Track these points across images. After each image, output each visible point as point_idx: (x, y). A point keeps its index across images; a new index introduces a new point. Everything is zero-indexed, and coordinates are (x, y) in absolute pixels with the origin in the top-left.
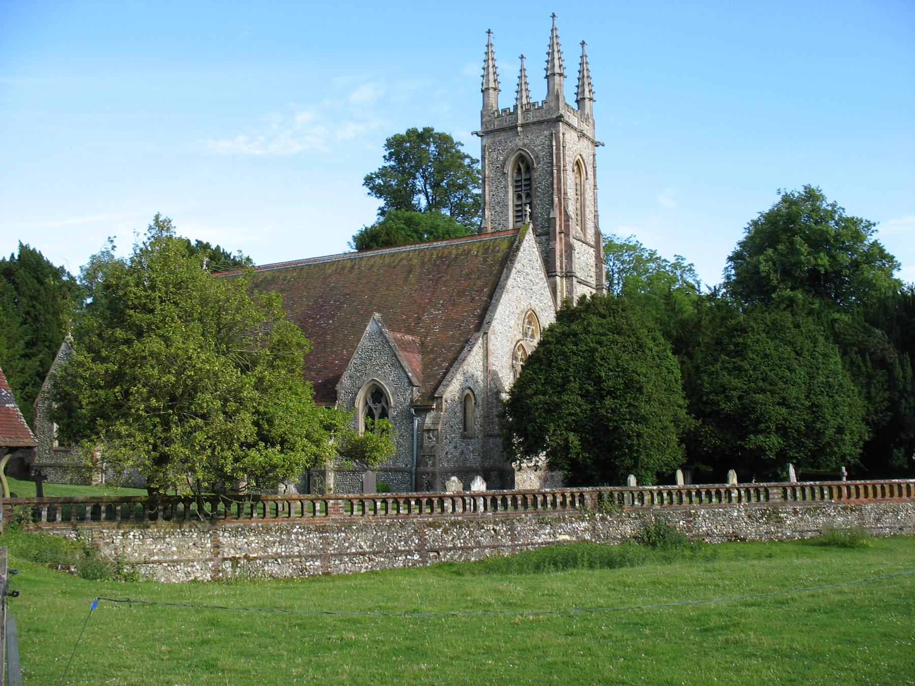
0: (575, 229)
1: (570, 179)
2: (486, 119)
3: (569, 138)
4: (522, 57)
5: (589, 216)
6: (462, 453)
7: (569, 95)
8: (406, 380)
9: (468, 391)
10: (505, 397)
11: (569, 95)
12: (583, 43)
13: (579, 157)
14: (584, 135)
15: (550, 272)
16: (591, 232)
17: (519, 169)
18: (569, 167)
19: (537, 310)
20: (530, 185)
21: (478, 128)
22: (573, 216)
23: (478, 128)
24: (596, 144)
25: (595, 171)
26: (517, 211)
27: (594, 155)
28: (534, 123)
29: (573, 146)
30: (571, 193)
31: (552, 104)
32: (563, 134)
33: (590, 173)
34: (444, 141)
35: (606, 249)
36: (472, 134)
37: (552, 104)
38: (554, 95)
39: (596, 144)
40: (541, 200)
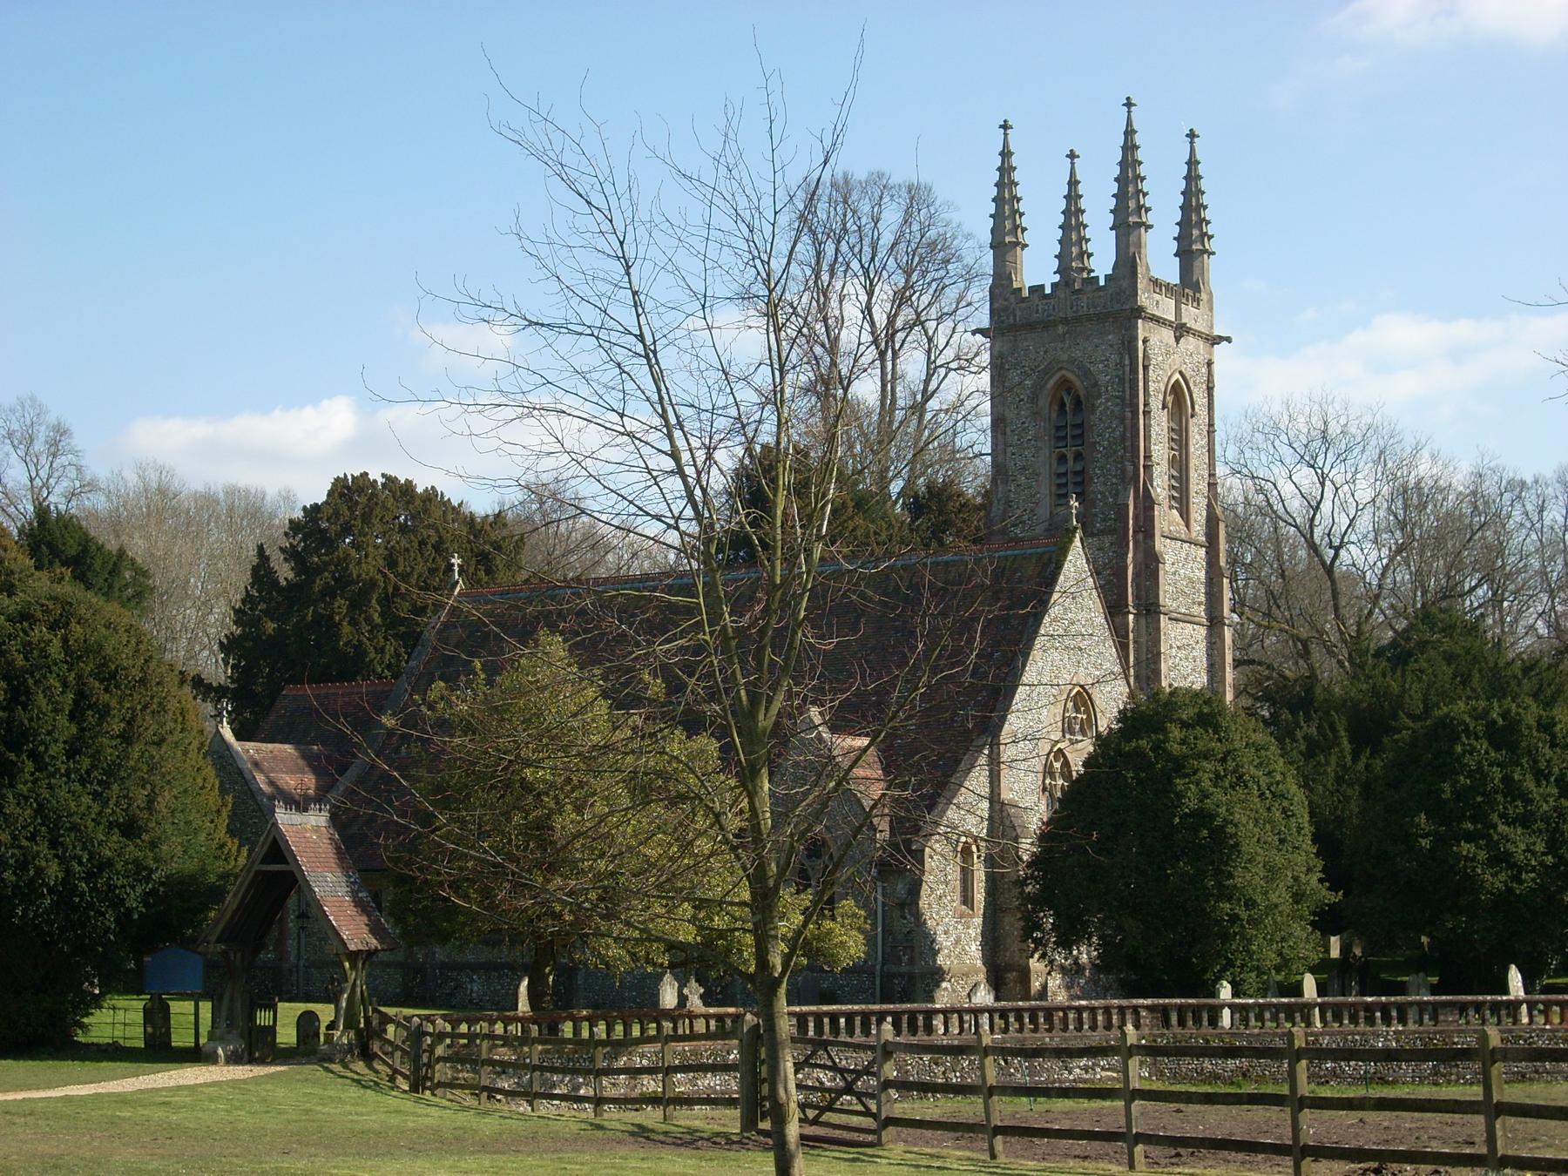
0: (1166, 518)
1: (1160, 424)
2: (996, 305)
3: (1155, 341)
4: (1072, 156)
6: (958, 941)
7: (1159, 256)
10: (1027, 847)
11: (1159, 256)
12: (1192, 135)
13: (1177, 376)
14: (1189, 331)
15: (1114, 609)
16: (1199, 515)
17: (1062, 404)
18: (1156, 404)
20: (1081, 436)
21: (985, 322)
23: (985, 322)
24: (1215, 340)
25: (1210, 389)
26: (1059, 486)
27: (1209, 364)
28: (1089, 318)
29: (1163, 357)
30: (1160, 451)
31: (1125, 284)
32: (1145, 341)
35: (1235, 537)
37: (1125, 284)
38: (1127, 263)
39: (1215, 340)
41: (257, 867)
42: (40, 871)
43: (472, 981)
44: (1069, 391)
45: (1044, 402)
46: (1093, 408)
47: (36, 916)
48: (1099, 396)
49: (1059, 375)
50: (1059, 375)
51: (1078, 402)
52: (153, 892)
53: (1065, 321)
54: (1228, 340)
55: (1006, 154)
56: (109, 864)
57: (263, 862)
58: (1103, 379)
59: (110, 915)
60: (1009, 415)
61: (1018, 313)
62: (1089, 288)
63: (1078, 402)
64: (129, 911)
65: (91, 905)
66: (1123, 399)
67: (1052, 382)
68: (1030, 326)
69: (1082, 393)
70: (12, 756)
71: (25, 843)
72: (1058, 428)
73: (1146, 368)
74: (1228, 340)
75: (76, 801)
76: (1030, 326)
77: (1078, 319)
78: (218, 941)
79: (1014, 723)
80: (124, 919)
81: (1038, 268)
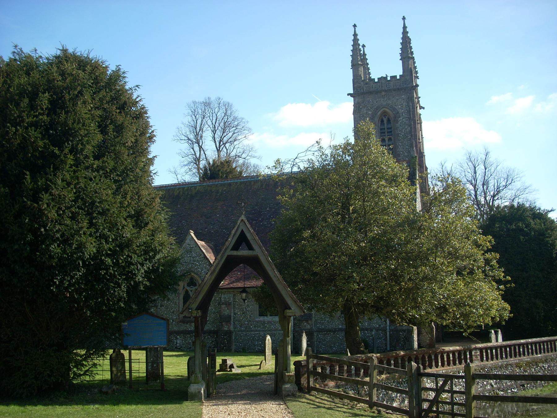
2: (355, 86)
17: (382, 121)
21: (352, 92)
23: (352, 92)
28: (395, 90)
31: (408, 78)
34: (228, 106)
36: (348, 95)
41: (229, 253)
42: (81, 247)
45: (376, 119)
46: (397, 122)
47: (70, 285)
48: (400, 117)
49: (382, 110)
50: (382, 110)
51: (389, 120)
52: (154, 270)
53: (385, 91)
56: (128, 244)
58: (401, 111)
59: (124, 288)
61: (365, 88)
62: (394, 79)
63: (389, 120)
64: (137, 284)
65: (113, 276)
66: (410, 118)
67: (380, 113)
68: (370, 93)
70: (56, 151)
71: (68, 222)
72: (381, 129)
75: (104, 190)
77: (390, 90)
78: (197, 309)
80: (133, 290)
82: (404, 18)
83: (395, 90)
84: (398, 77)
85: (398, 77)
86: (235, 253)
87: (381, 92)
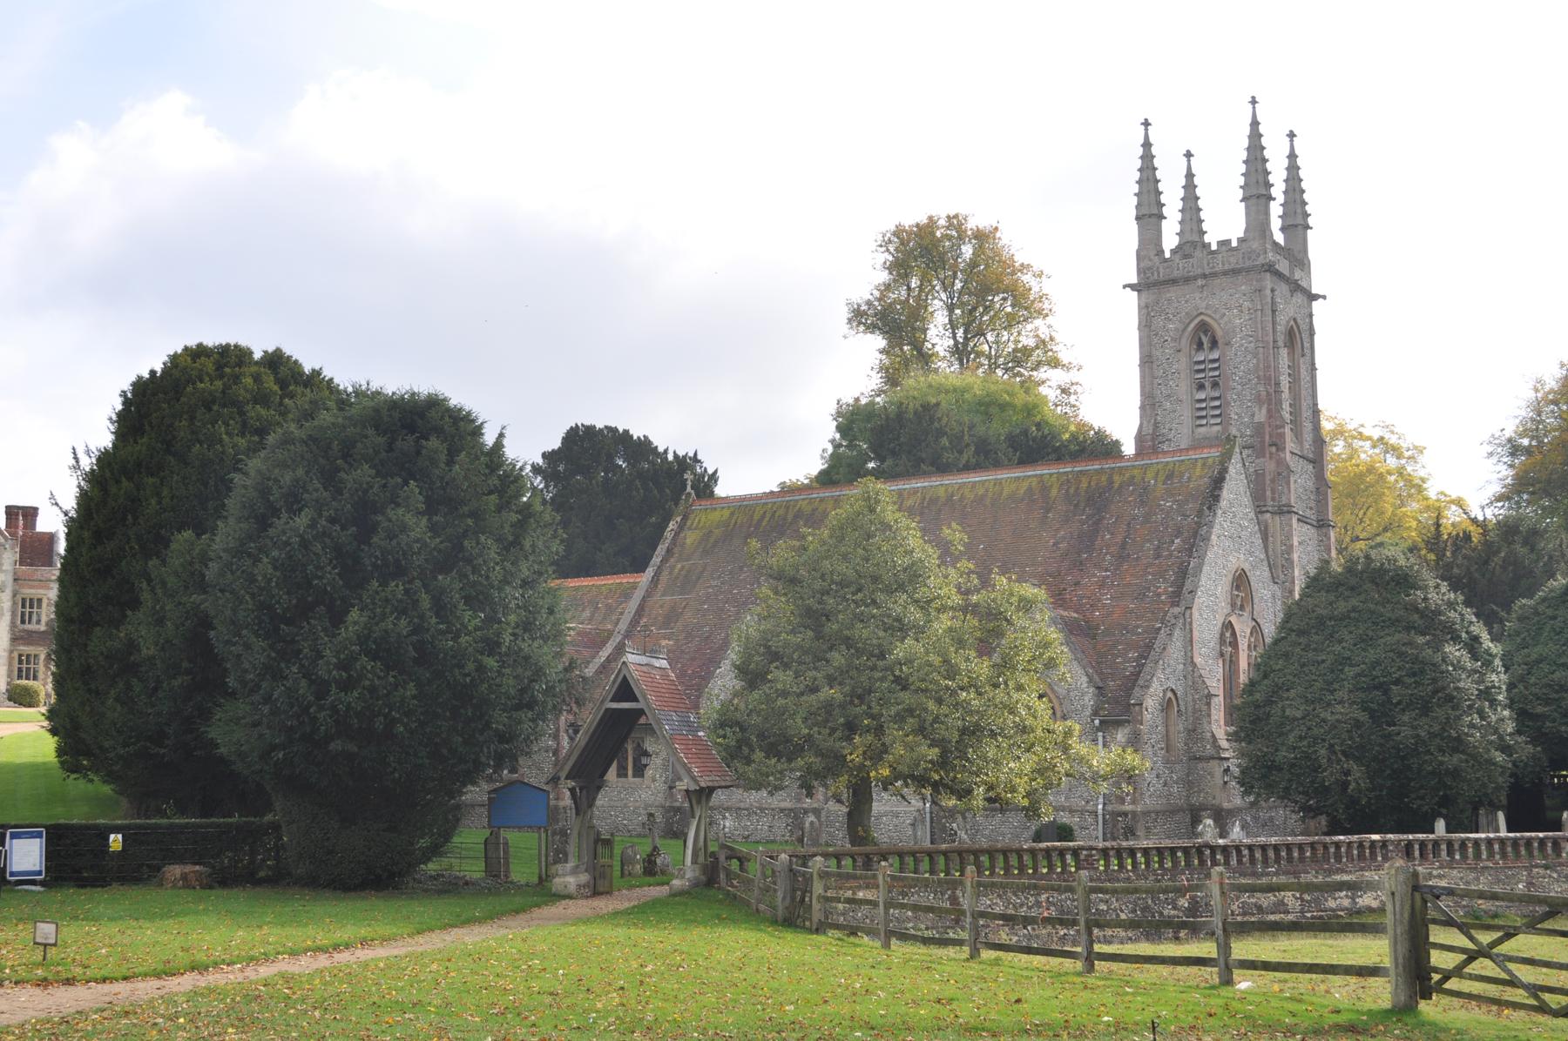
5: (1306, 414)
8: (1085, 679)
9: (1169, 694)
12: (1292, 135)
16: (1308, 437)
17: (1200, 346)
19: (1246, 567)
21: (1134, 280)
22: (1287, 417)
23: (1134, 280)
28: (1225, 273)
32: (1273, 291)
33: (1307, 345)
40: (1238, 395)
43: (724, 818)
44: (1205, 333)
53: (1204, 276)
54: (1324, 297)
55: (1147, 145)
57: (612, 700)
60: (1157, 353)
63: (1214, 343)
68: (1174, 282)
69: (1219, 333)
73: (1274, 311)
74: (1324, 297)
76: (1174, 282)
77: (1214, 275)
79: (1201, 599)
81: (1170, 238)
82: (1254, 101)
83: (1225, 273)
84: (1234, 244)
85: (1234, 244)
86: (615, 705)
87: (1195, 278)
